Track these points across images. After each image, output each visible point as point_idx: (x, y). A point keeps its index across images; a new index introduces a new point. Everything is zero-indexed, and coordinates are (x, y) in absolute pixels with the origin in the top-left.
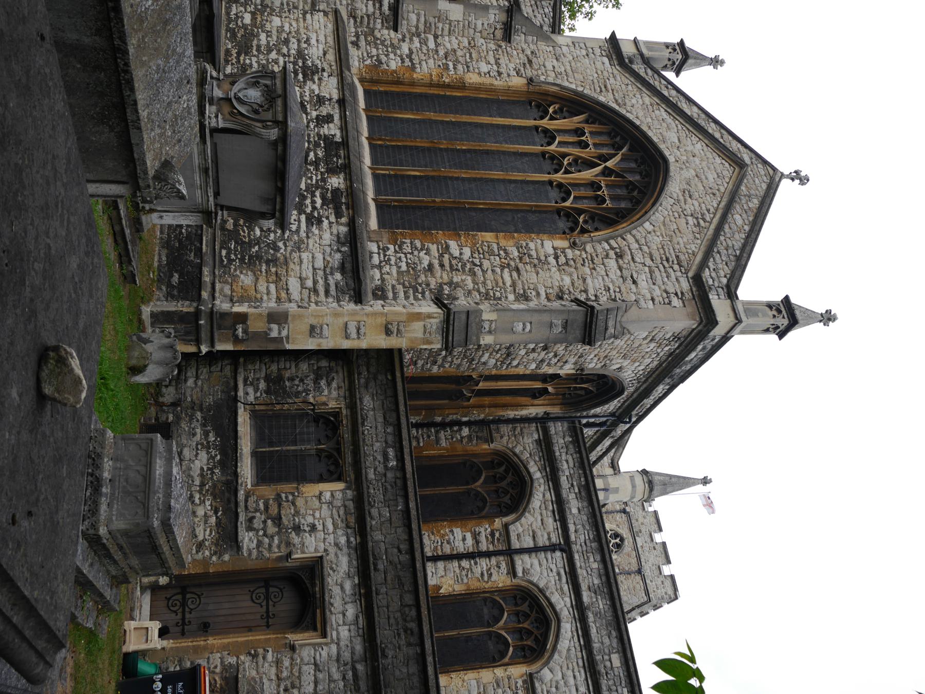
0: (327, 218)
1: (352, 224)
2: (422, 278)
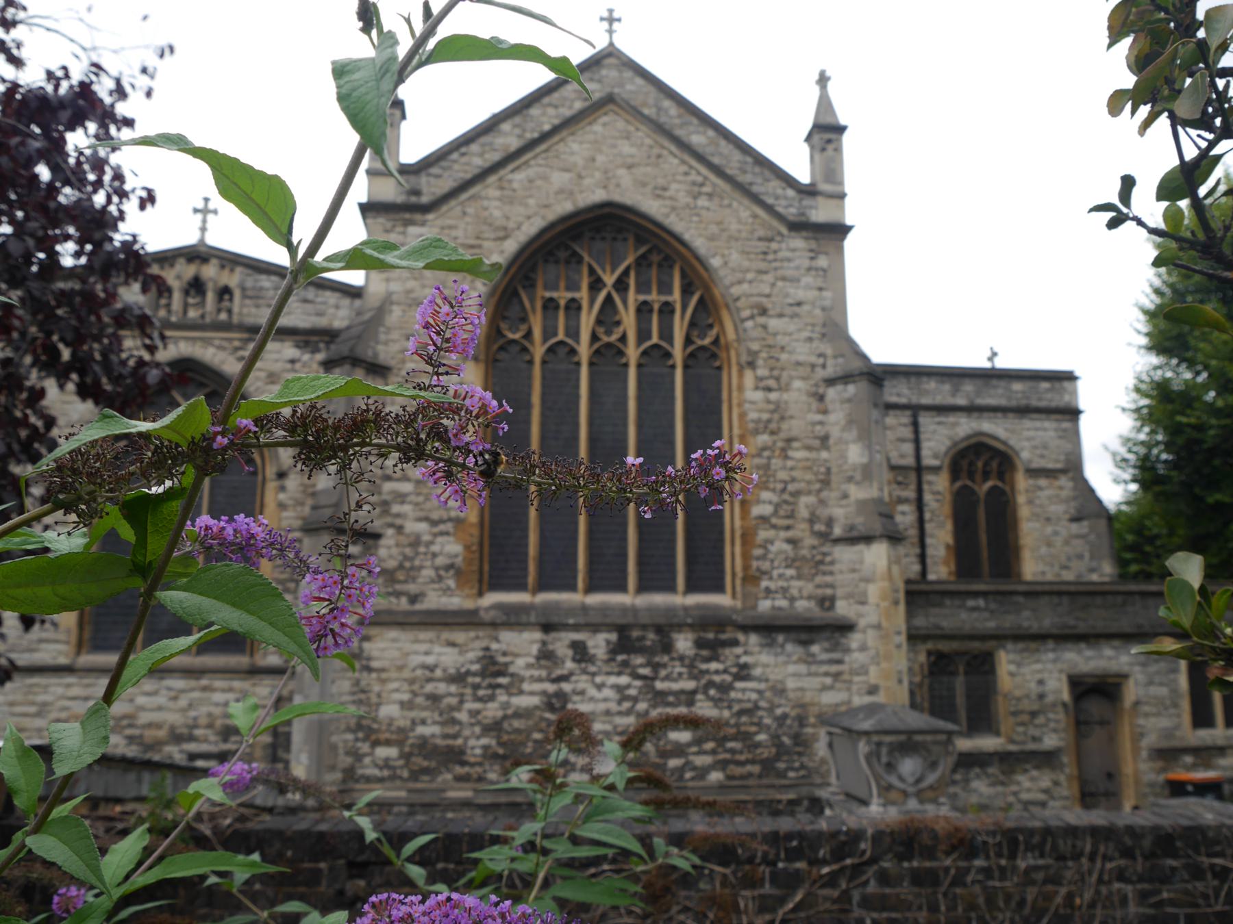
0: (738, 657)
1: (746, 628)
2: (805, 552)
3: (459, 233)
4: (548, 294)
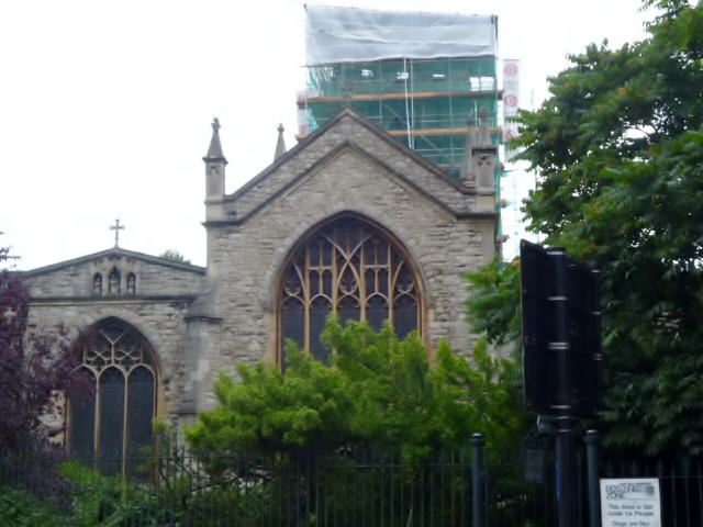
3: (259, 236)
4: (313, 268)
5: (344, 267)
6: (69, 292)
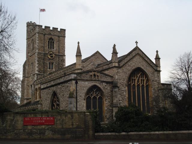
5: (138, 78)
6: (85, 79)
